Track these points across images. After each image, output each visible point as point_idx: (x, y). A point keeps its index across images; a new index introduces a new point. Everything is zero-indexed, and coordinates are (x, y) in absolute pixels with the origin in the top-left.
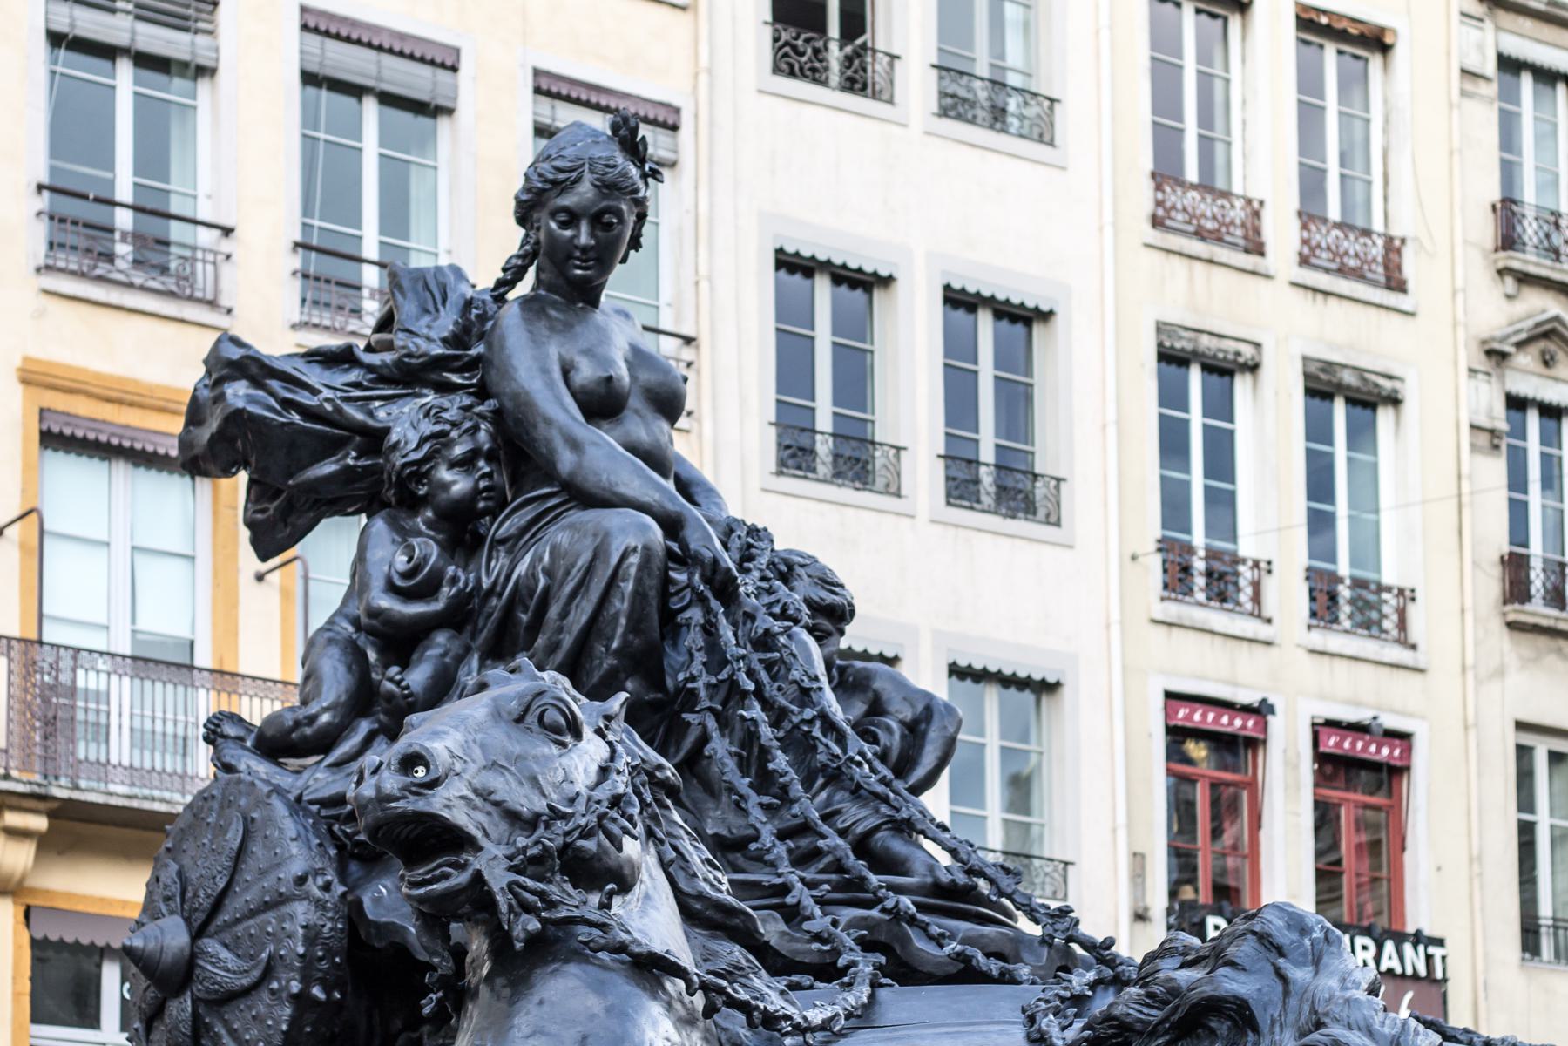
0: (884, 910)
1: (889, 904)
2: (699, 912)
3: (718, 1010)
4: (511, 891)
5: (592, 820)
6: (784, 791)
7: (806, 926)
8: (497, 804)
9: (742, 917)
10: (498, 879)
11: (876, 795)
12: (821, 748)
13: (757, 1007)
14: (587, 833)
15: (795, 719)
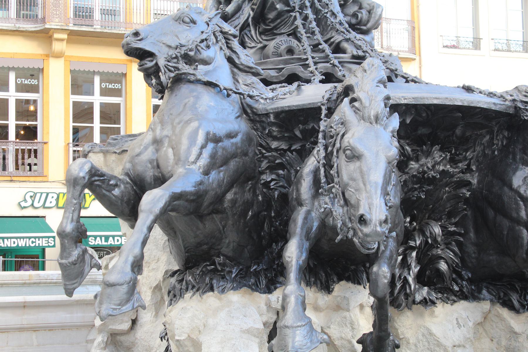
0: (331, 64)
1: (332, 62)
2: (242, 68)
3: (230, 95)
4: (166, 67)
5: (194, 46)
6: (313, 33)
7: (309, 69)
8: (164, 44)
9: (255, 69)
10: (162, 63)
11: (342, 32)
12: (329, 20)
13: (245, 94)
14: (191, 50)
15: (323, 12)
